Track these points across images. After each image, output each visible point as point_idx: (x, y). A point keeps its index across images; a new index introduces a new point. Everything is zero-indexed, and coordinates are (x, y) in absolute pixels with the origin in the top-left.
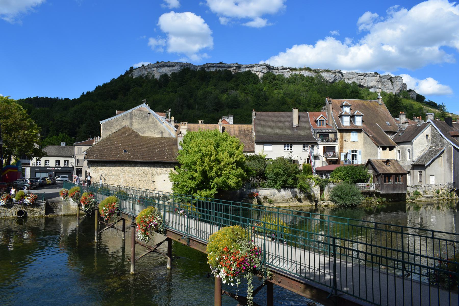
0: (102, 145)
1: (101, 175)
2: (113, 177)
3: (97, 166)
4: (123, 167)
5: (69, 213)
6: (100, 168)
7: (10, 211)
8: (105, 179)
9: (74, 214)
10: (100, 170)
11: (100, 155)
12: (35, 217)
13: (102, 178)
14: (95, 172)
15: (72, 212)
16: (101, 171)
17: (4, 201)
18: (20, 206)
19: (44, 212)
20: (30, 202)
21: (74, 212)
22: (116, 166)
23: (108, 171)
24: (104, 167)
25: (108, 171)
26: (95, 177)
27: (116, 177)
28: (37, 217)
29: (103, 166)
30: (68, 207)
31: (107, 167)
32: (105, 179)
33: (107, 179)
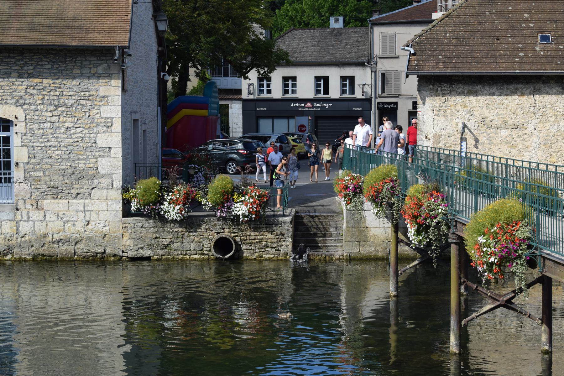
0: (465, 21)
1: (465, 126)
2: (504, 133)
3: (450, 94)
4: (537, 97)
5: (365, 250)
6: (459, 99)
7: (196, 239)
8: (477, 141)
9: (380, 254)
10: (458, 108)
11: (458, 55)
12: (266, 260)
13: (468, 135)
14: (445, 117)
15: (372, 249)
16: (463, 112)
17: (178, 207)
18: (221, 222)
19: (290, 247)
20: (250, 212)
21: (379, 249)
22: (513, 93)
23: (486, 112)
24: (473, 99)
25: (486, 112)
26: (443, 133)
27: (514, 132)
28: (269, 260)
29: (470, 93)
30: (362, 231)
31: (481, 99)
32: (477, 141)
33: (482, 139)
